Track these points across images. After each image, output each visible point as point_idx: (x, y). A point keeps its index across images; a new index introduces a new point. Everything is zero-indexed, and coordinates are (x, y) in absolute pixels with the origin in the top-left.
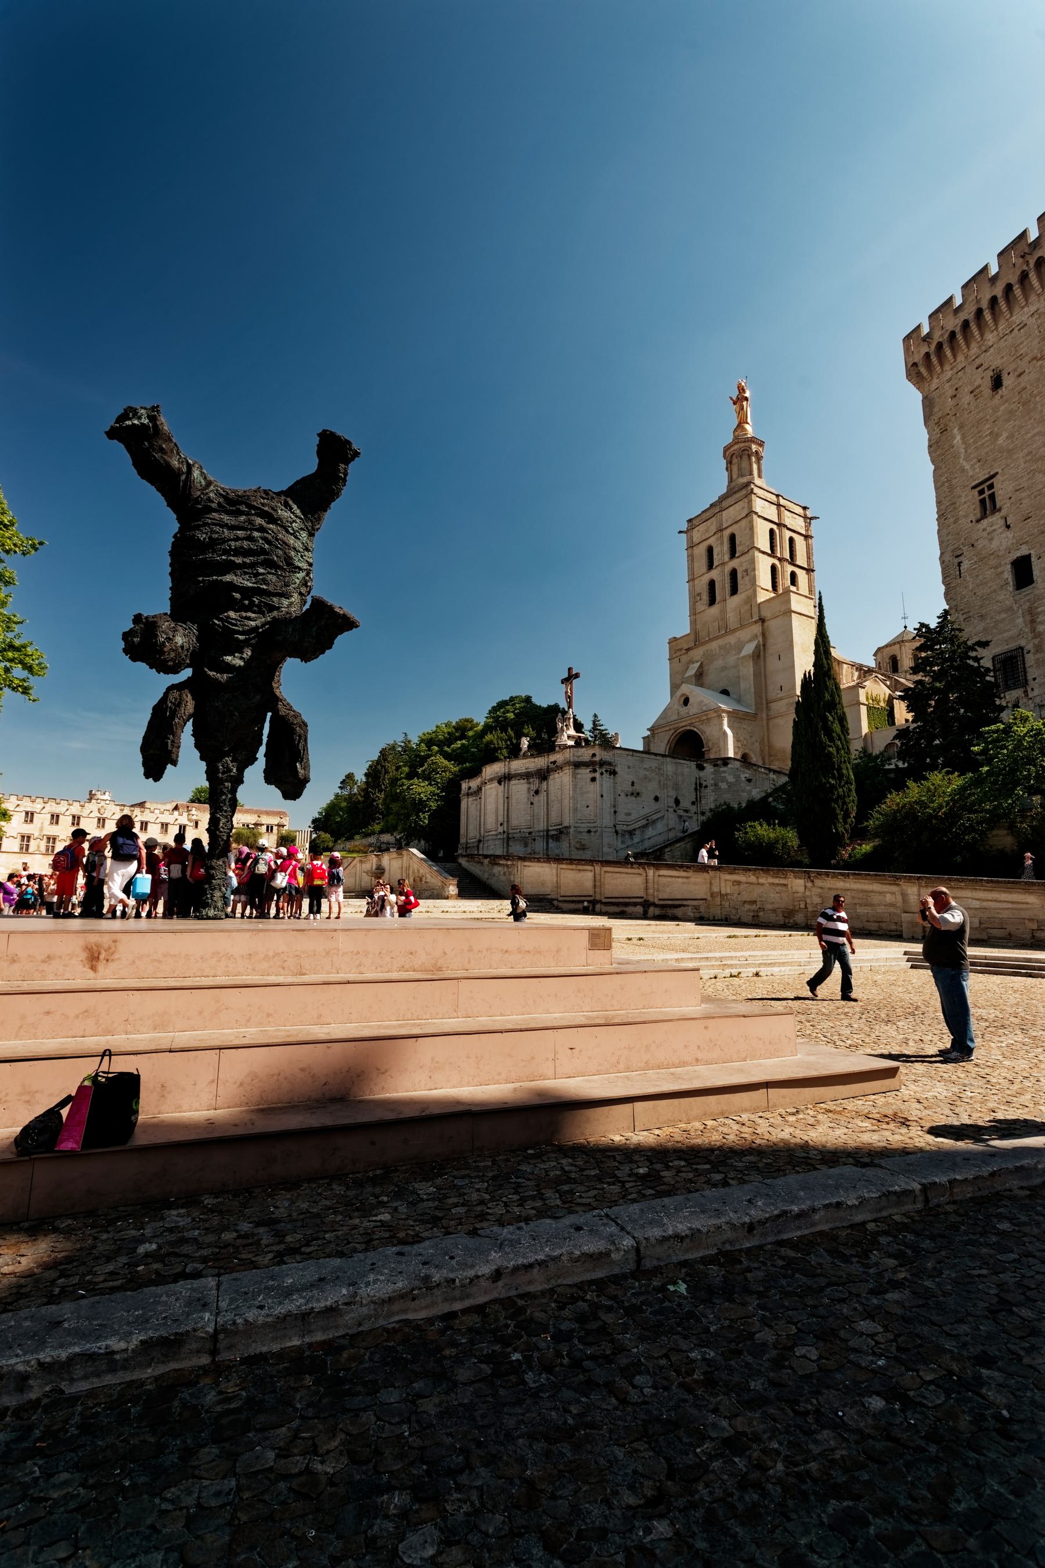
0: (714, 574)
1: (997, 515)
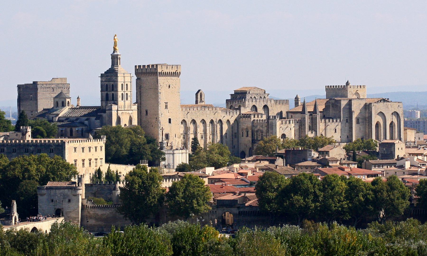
1: (167, 110)
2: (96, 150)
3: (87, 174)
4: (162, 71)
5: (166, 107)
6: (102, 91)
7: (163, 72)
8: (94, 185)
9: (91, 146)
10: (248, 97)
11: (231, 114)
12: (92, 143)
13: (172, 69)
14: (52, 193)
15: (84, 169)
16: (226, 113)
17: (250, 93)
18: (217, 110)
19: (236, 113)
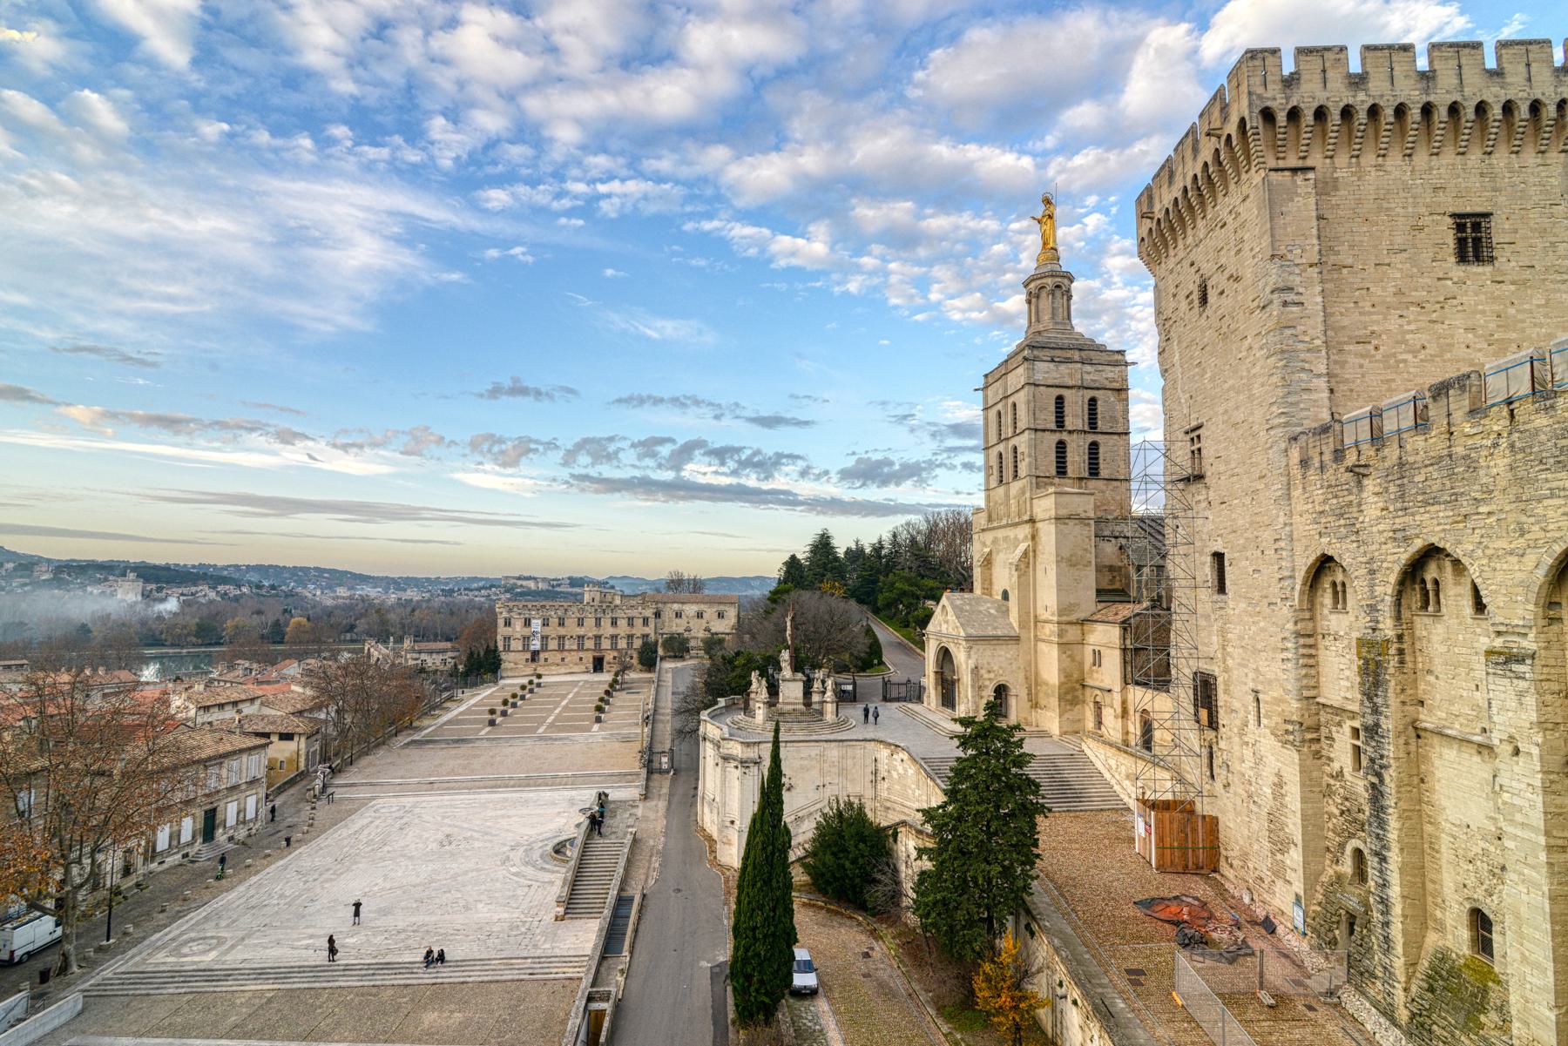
0: (1001, 447)
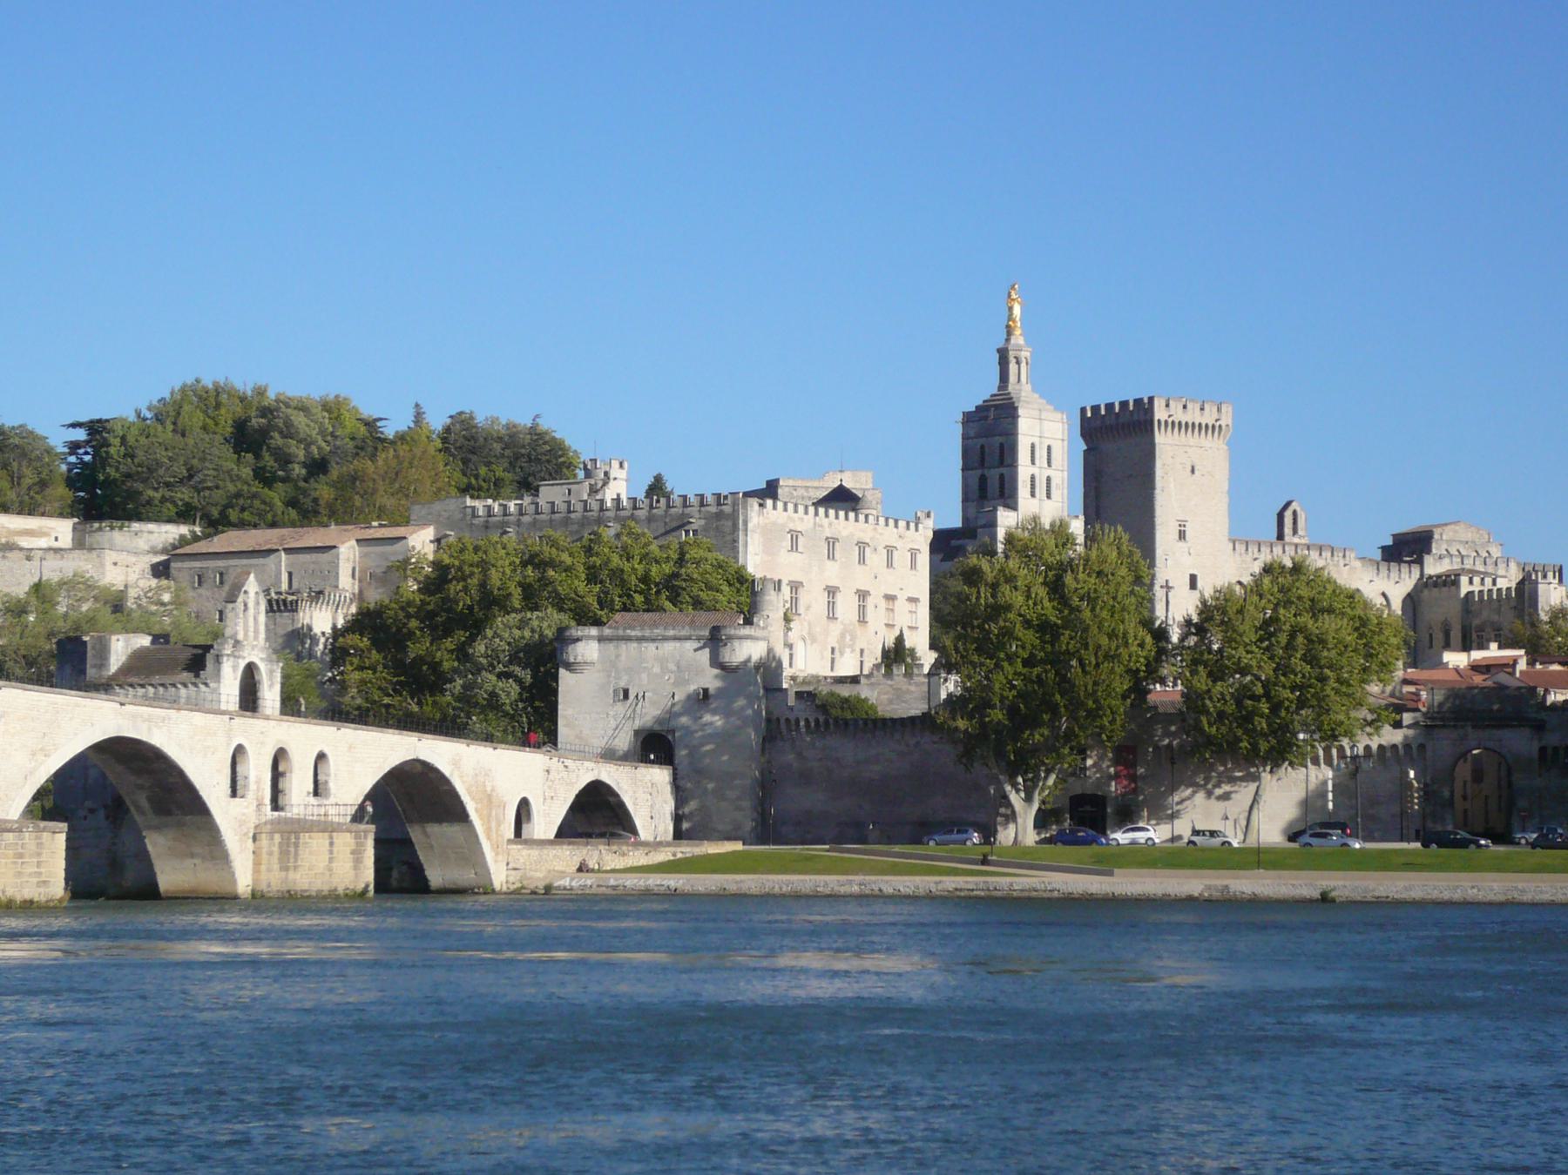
2: (890, 564)
3: (848, 650)
4: (1170, 416)
5: (1182, 535)
6: (965, 468)
7: (1173, 423)
8: (863, 680)
9: (867, 541)
10: (1437, 549)
11: (1392, 575)
12: (875, 529)
13: (1202, 415)
14: (623, 658)
15: (835, 629)
16: (1378, 569)
17: (1444, 537)
18: (1347, 558)
19: (1410, 572)
